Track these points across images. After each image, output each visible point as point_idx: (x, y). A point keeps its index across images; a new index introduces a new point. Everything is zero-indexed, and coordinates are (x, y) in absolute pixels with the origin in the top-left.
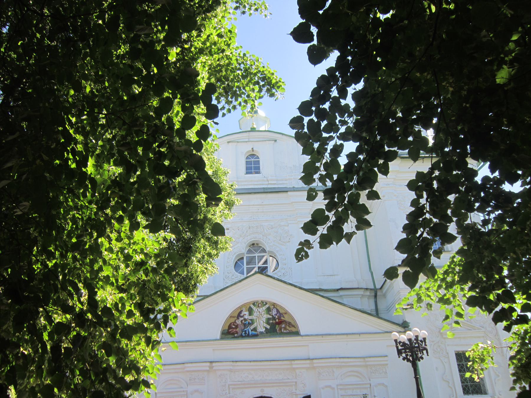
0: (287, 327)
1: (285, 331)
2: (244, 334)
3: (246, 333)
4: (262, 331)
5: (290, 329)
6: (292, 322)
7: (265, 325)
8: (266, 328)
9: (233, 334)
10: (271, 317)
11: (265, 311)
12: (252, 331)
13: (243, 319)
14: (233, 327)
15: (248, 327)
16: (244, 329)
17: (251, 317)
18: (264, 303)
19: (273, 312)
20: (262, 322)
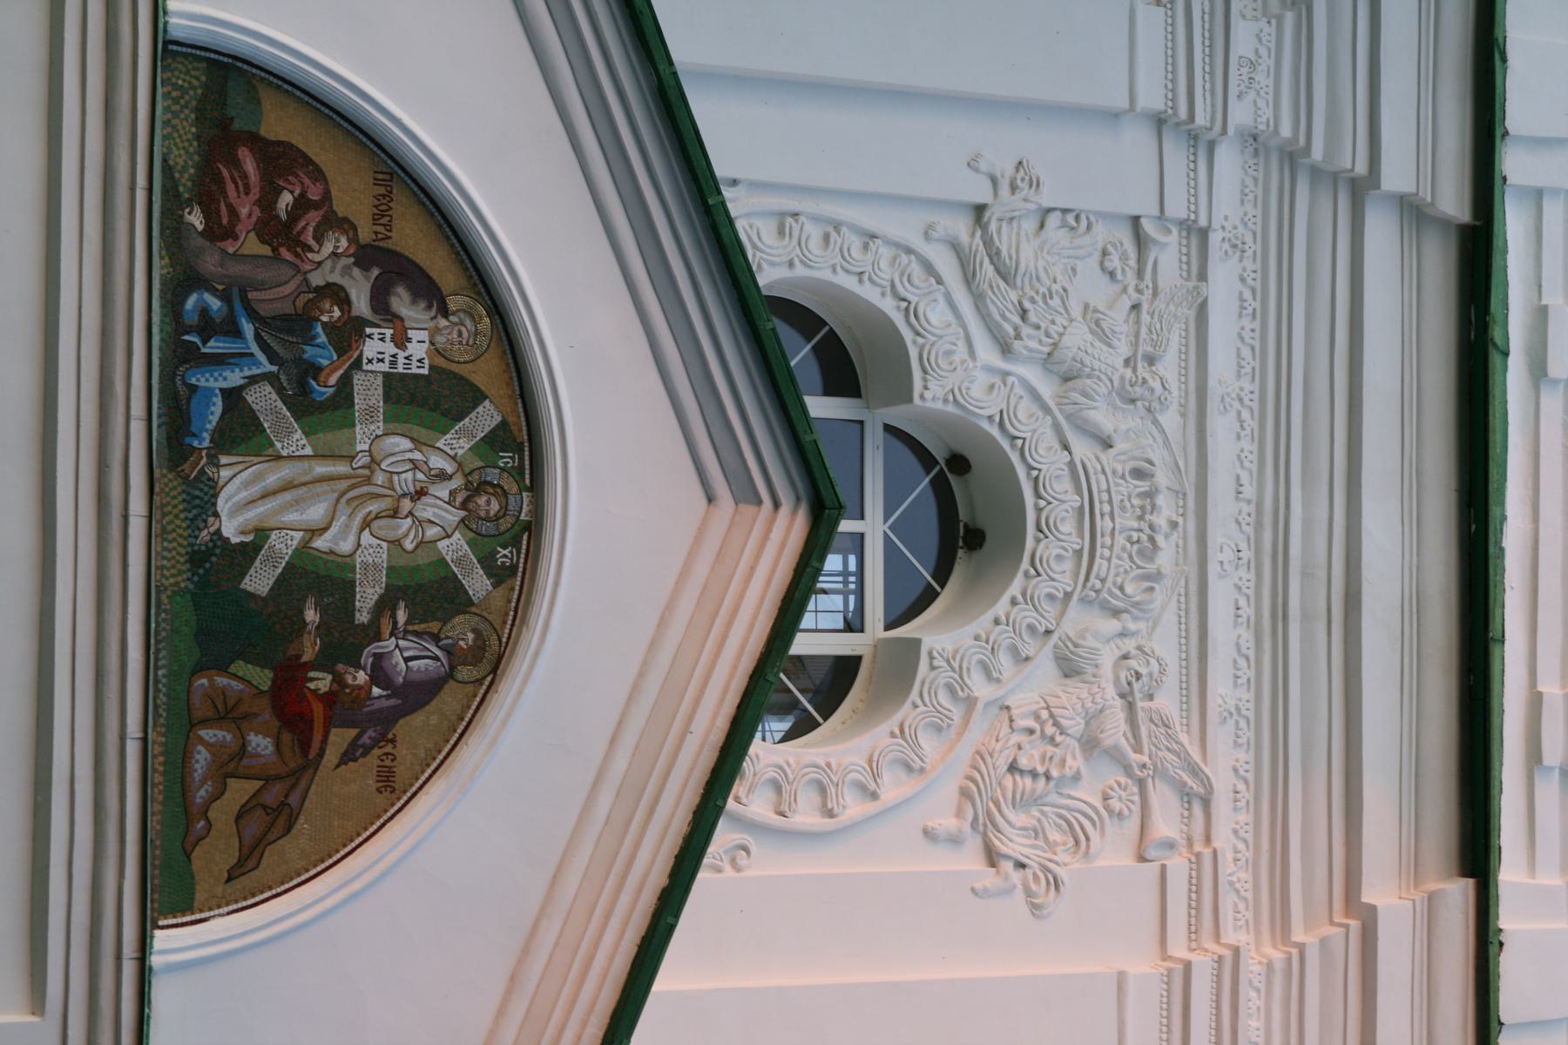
0: (240, 791)
1: (201, 758)
2: (204, 311)
3: (207, 326)
4: (222, 505)
5: (223, 813)
6: (289, 848)
7: (284, 545)
8: (247, 553)
9: (208, 198)
10: (363, 617)
11: (423, 558)
12: (233, 397)
13: (361, 304)
14: (286, 199)
15: (272, 357)
16: (253, 315)
17: (368, 393)
18: (504, 555)
19: (410, 646)
20: (316, 513)
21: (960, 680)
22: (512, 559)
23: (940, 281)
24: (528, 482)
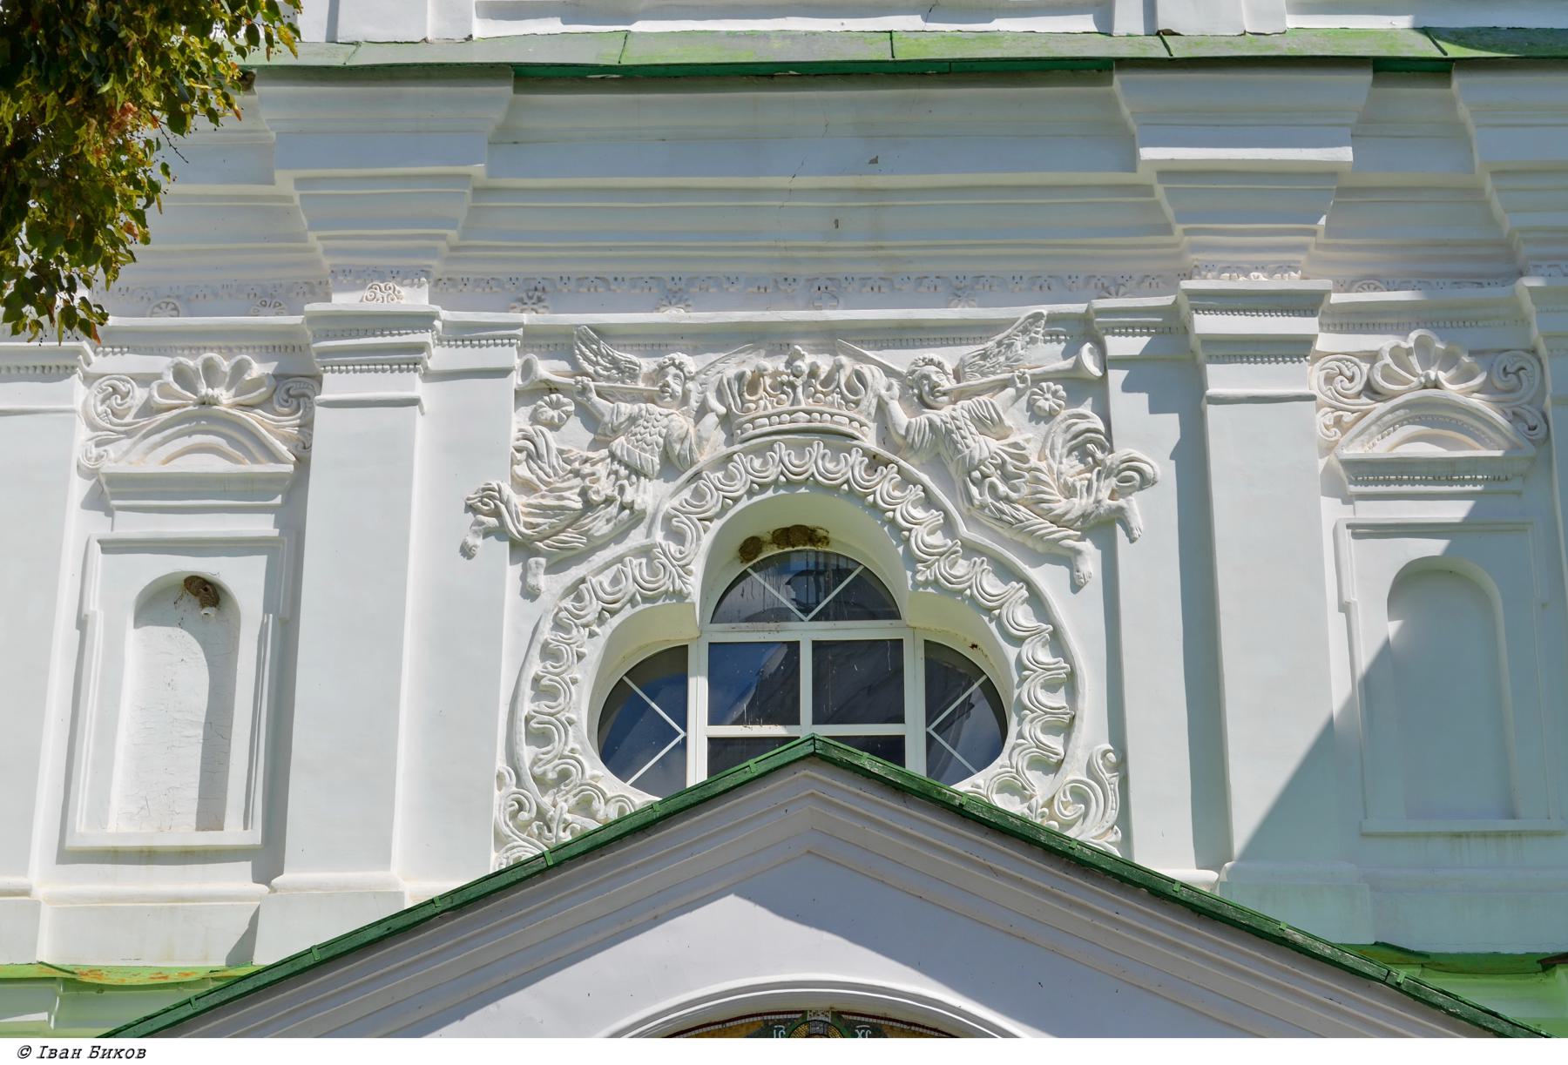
21: (947, 554)
22: (866, 1029)
23: (583, 581)
24: (798, 1016)
